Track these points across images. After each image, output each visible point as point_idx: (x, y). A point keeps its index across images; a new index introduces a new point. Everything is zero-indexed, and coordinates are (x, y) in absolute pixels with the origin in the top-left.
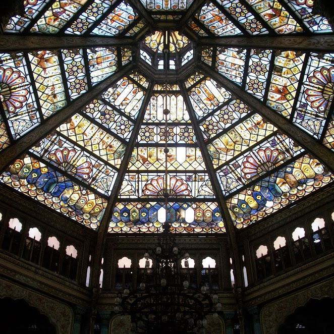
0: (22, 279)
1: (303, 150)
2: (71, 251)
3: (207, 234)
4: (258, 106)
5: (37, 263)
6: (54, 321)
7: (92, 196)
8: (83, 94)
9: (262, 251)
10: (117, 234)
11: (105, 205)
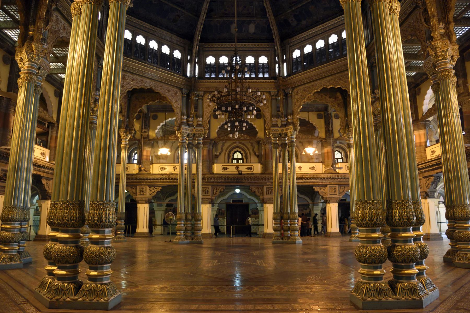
2: (177, 54)
6: (171, 98)
9: (296, 54)
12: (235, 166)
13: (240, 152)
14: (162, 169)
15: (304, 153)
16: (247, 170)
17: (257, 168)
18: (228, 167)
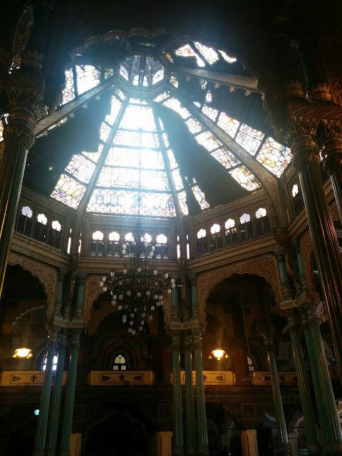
0: (17, 249)
1: (240, 162)
3: (162, 217)
4: (211, 125)
5: (29, 236)
6: (43, 280)
7: (74, 183)
8: (71, 102)
9: (202, 234)
10: (92, 213)
11: (84, 191)
12: (119, 375)
13: (123, 355)
14: (15, 379)
15: (227, 356)
16: (133, 380)
17: (149, 377)
18: (109, 376)
